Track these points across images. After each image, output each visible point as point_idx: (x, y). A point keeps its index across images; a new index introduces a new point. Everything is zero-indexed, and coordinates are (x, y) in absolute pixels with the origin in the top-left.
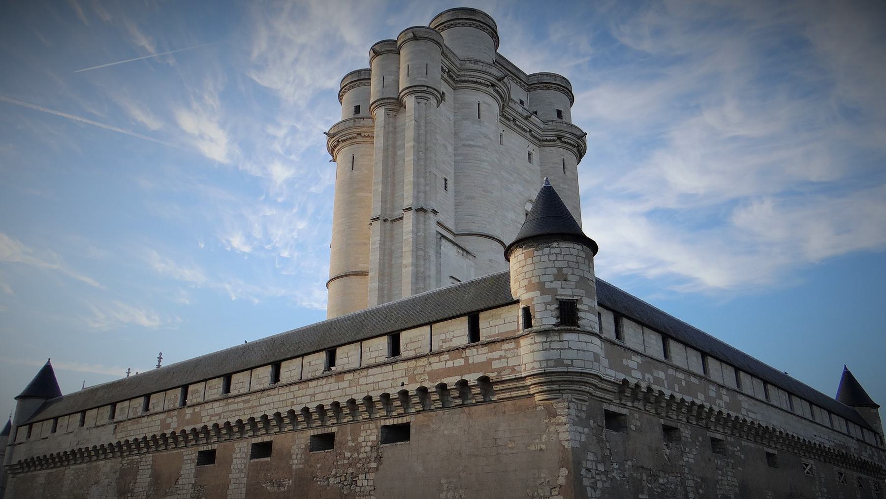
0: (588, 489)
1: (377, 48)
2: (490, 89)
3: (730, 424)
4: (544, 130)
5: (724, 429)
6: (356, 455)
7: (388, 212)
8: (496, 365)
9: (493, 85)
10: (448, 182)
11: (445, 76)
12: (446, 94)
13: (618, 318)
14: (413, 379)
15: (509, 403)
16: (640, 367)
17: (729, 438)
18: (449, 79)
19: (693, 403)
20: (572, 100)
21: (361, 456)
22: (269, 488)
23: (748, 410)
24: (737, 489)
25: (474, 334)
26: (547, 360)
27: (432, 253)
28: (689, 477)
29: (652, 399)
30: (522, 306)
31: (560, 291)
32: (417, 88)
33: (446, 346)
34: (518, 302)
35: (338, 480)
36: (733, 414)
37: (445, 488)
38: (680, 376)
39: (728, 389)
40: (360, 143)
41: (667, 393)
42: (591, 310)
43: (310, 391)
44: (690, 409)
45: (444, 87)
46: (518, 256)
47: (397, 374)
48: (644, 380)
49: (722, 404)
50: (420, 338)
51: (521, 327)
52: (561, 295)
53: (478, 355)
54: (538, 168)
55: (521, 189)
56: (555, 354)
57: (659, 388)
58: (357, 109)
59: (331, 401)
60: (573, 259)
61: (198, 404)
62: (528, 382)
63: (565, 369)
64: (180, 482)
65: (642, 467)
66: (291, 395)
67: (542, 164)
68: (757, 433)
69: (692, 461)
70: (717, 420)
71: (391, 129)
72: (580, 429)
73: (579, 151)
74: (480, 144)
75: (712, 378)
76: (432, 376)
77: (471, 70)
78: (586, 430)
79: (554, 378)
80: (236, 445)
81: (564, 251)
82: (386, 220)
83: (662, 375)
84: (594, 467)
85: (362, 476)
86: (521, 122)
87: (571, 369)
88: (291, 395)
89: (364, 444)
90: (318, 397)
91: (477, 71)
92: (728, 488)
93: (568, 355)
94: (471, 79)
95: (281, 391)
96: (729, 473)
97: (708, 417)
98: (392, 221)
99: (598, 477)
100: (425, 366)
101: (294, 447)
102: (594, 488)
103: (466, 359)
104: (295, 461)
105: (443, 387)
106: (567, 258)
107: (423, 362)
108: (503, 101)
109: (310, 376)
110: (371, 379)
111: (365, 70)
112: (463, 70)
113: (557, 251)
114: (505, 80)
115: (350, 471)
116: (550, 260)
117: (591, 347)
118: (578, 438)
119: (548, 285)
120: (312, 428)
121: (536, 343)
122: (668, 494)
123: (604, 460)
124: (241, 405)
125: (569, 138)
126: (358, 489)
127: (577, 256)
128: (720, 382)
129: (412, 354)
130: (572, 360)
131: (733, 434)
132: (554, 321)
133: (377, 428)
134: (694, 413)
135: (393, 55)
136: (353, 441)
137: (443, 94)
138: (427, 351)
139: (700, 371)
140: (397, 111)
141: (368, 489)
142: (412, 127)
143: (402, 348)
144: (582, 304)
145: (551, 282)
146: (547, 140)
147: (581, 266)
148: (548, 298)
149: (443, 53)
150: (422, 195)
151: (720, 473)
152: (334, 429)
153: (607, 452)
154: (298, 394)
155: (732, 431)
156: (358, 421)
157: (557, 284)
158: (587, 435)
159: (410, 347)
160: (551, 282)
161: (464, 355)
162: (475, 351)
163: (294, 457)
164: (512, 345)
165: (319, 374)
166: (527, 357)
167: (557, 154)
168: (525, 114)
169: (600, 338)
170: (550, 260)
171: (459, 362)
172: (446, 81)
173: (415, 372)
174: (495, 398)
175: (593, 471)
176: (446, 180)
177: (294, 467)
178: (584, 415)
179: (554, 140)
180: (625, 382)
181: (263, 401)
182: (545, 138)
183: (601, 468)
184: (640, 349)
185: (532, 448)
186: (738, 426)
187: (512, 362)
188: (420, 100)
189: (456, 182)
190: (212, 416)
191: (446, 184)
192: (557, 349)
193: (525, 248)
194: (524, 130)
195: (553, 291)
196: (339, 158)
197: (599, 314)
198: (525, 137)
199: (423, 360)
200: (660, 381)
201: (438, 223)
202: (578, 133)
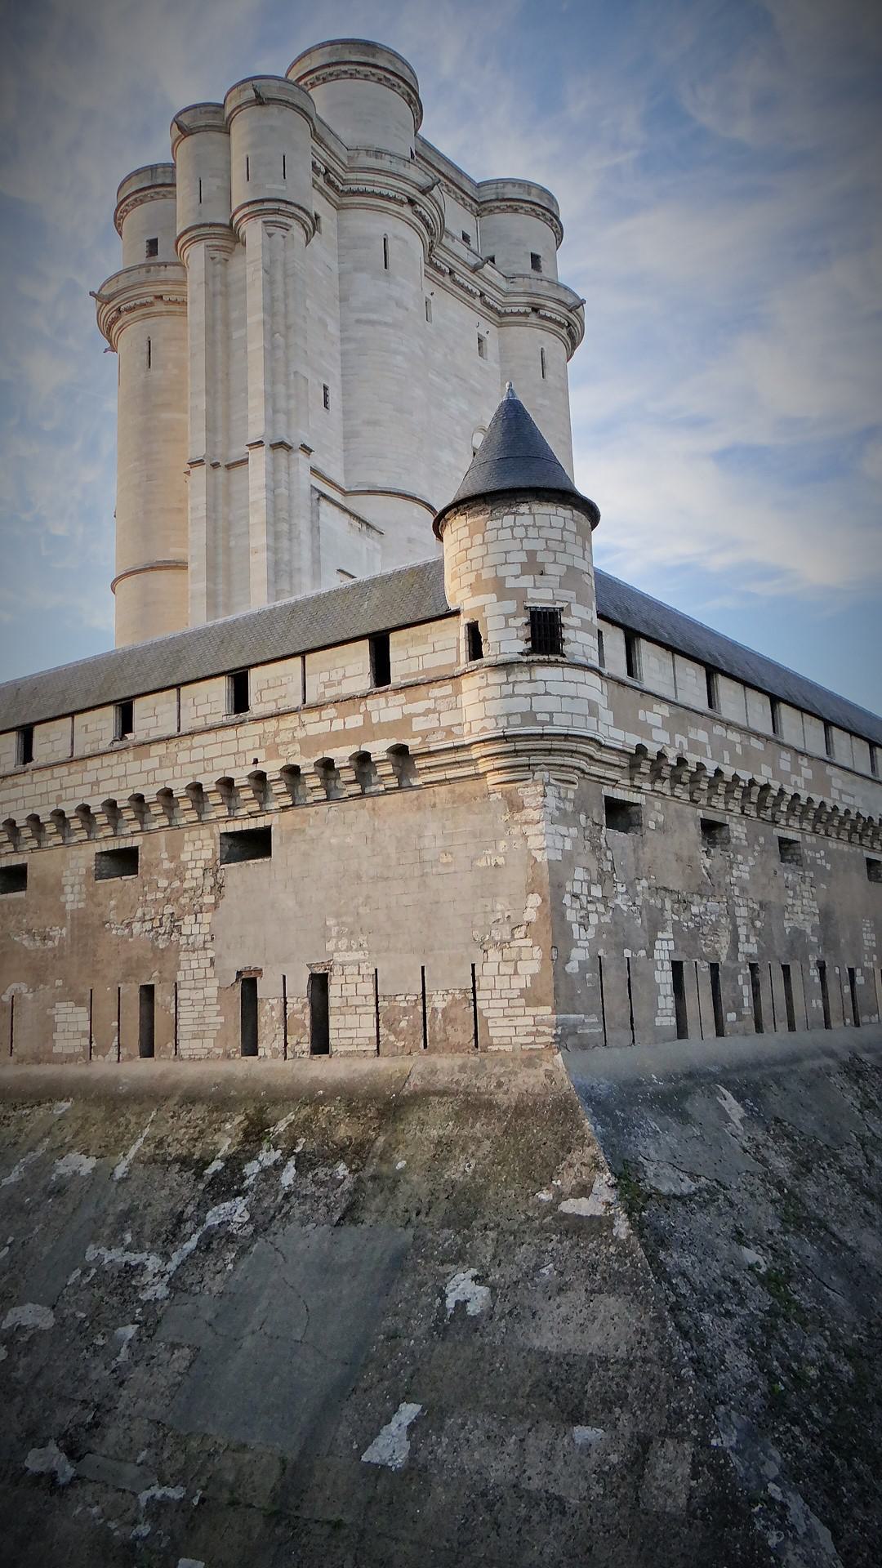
0: (575, 927)
1: (185, 120)
2: (407, 211)
3: (811, 815)
4: (507, 294)
5: (801, 822)
6: (177, 884)
7: (219, 451)
8: (419, 725)
9: (412, 202)
10: (330, 392)
11: (321, 180)
12: (324, 219)
13: (632, 637)
14: (273, 752)
15: (443, 789)
16: (667, 724)
17: (808, 838)
18: (326, 188)
19: (752, 782)
20: (559, 235)
21: (186, 885)
22: (25, 943)
23: (841, 792)
24: (817, 919)
25: (381, 673)
26: (508, 715)
27: (303, 526)
28: (740, 902)
29: (685, 778)
30: (464, 620)
31: (531, 593)
32: (267, 205)
33: (331, 693)
34: (457, 613)
35: (148, 926)
36: (817, 799)
37: (334, 934)
38: (734, 737)
39: (811, 757)
40: (160, 314)
41: (711, 767)
42: (585, 626)
43: (90, 777)
44: (746, 793)
45: (318, 204)
46: (458, 528)
47: (245, 745)
48: (672, 745)
49: (799, 782)
50: (284, 680)
51: (464, 656)
52: (533, 600)
53: (387, 708)
54: (497, 366)
55: (465, 407)
56: (522, 705)
57: (698, 759)
58: (153, 246)
59: (130, 793)
60: (556, 535)
62: (475, 753)
63: (538, 730)
65: (665, 889)
66: (56, 785)
67: (503, 357)
68: (854, 828)
69: (746, 876)
70: (791, 809)
71: (219, 287)
72: (563, 830)
73: (570, 334)
74: (389, 320)
75: (786, 741)
76: (307, 744)
77: (369, 170)
78: (574, 831)
79: (520, 746)
81: (540, 521)
82: (215, 465)
83: (702, 736)
84: (585, 892)
86: (464, 276)
87: (548, 730)
88: (56, 785)
89: (191, 865)
90: (104, 787)
91: (379, 171)
92: (802, 917)
93: (542, 705)
94: (369, 189)
95: (37, 776)
96: (806, 894)
97: (776, 805)
98: (228, 467)
99: (591, 907)
100: (295, 729)
101: (68, 873)
102: (584, 925)
103: (367, 715)
104: (70, 897)
105: (327, 765)
106: (545, 533)
107: (291, 721)
108: (432, 234)
109: (88, 751)
110: (197, 754)
111: (164, 165)
112: (352, 170)
113: (527, 520)
114: (435, 192)
115: (169, 909)
116: (514, 538)
117: (583, 691)
118: (559, 845)
119: (510, 583)
121: (488, 685)
122: (706, 930)
123: (602, 878)
125: (553, 310)
126: (183, 940)
127: (563, 529)
128: (800, 746)
129: (271, 708)
130: (551, 714)
131: (815, 832)
132: (524, 646)
133: (212, 837)
134: (754, 799)
136: (172, 859)
137: (317, 217)
138: (297, 702)
139: (767, 730)
140: (229, 251)
141: (201, 938)
142: (259, 283)
143: (252, 699)
144: (569, 615)
145: (517, 577)
146: (513, 314)
147: (571, 548)
148: (511, 606)
149: (315, 134)
150: (281, 417)
151: (791, 893)
152: (137, 841)
153: (607, 866)
154: (67, 781)
155: (814, 828)
156: (179, 827)
157: (526, 581)
158: (574, 840)
159: (267, 695)
160: (517, 577)
161: (362, 709)
162: (382, 700)
163: (68, 889)
164: (448, 689)
165: (104, 746)
166: (475, 708)
167: (531, 338)
168: (473, 260)
169: (601, 674)
170: (514, 538)
171: (355, 721)
172: (321, 191)
173: (278, 740)
174: (416, 782)
175: (583, 898)
176: (325, 388)
177: (68, 907)
178: (569, 807)
179: (526, 314)
180: (641, 749)
182: (508, 310)
183: (597, 892)
184: (668, 693)
185: (482, 863)
186: (824, 817)
187: (447, 719)
188: (272, 230)
189: (346, 393)
191: (326, 396)
192: (526, 696)
193: (472, 515)
194: (470, 292)
195: (519, 594)
196: (123, 343)
197: (600, 633)
198: (472, 307)
199: (292, 717)
200: (700, 746)
201: (314, 471)
202: (570, 300)
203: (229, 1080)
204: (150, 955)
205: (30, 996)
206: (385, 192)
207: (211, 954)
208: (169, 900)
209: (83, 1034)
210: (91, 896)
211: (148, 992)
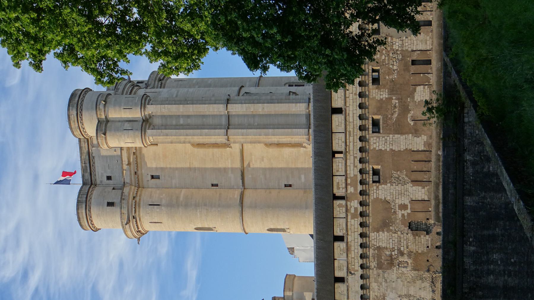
6: (384, 52)
22: (396, 116)
35: (395, 62)
40: (140, 200)
61: (346, 180)
64: (388, 198)
74: (176, 92)
80: (372, 148)
85: (394, 48)
88: (351, 95)
95: (348, 105)
98: (229, 125)
120: (368, 84)
124: (351, 138)
126: (400, 49)
135: (109, 124)
163: (381, 97)
177: (387, 97)
179: (161, 83)
181: (351, 120)
190: (355, 166)
203: (438, 26)
204: (403, 62)
205: (412, 112)
206: (130, 89)
207: (404, 38)
208: (388, 55)
209: (424, 88)
210: (384, 87)
211: (414, 62)
